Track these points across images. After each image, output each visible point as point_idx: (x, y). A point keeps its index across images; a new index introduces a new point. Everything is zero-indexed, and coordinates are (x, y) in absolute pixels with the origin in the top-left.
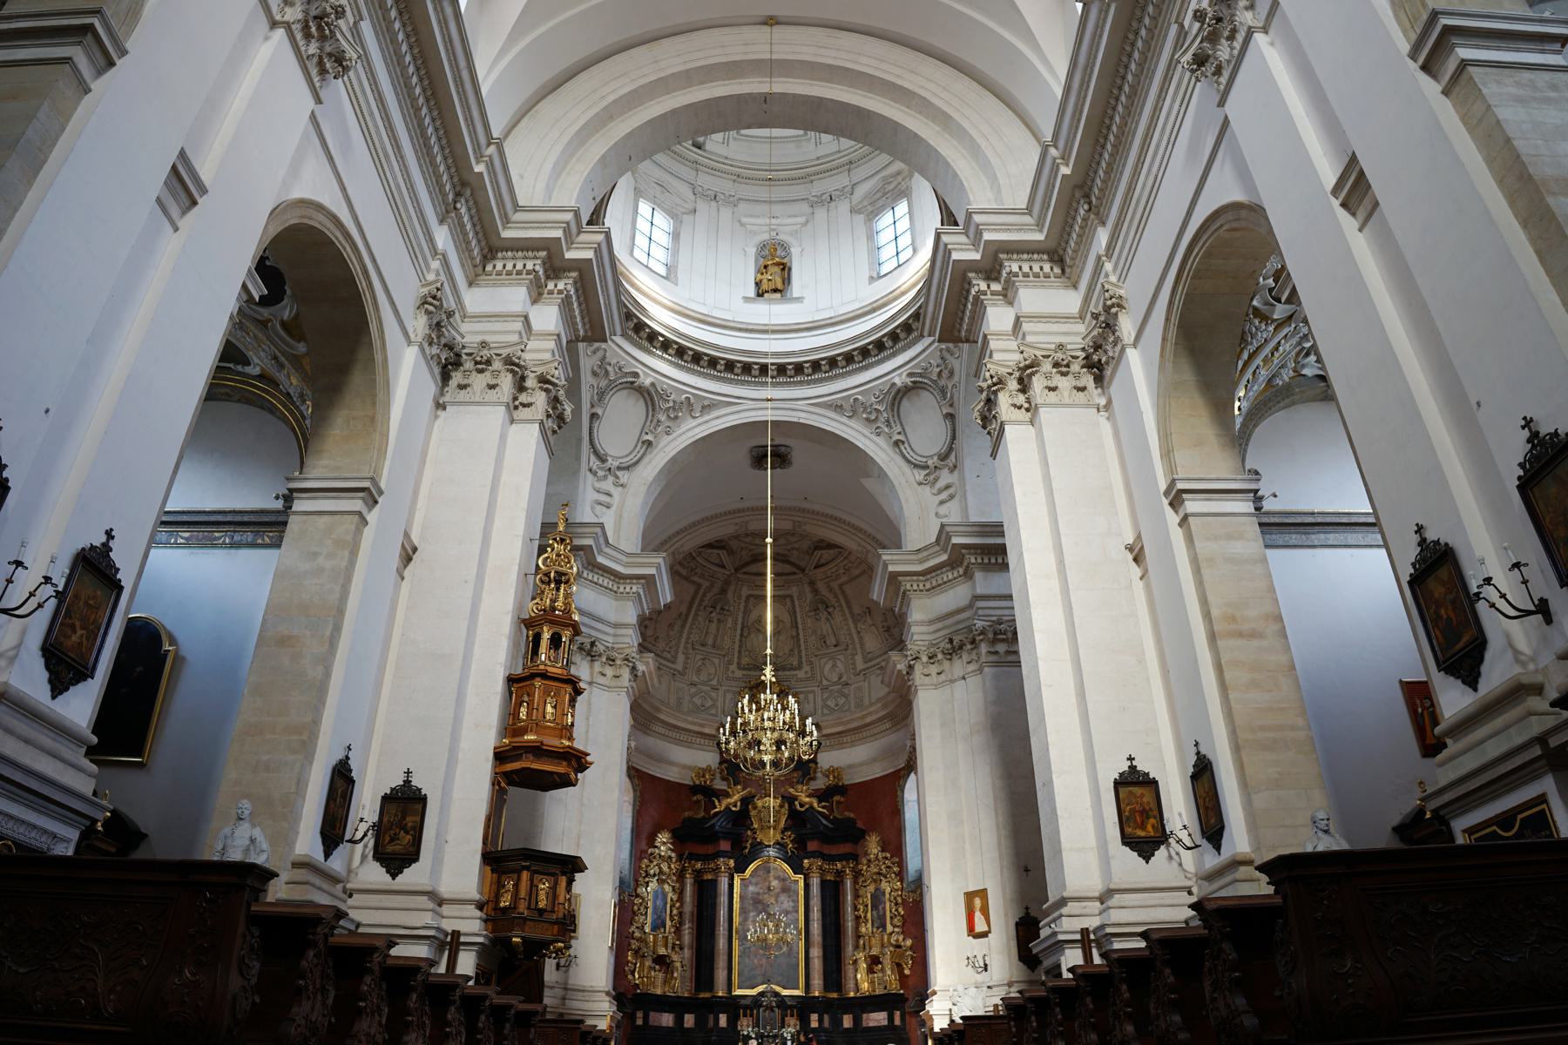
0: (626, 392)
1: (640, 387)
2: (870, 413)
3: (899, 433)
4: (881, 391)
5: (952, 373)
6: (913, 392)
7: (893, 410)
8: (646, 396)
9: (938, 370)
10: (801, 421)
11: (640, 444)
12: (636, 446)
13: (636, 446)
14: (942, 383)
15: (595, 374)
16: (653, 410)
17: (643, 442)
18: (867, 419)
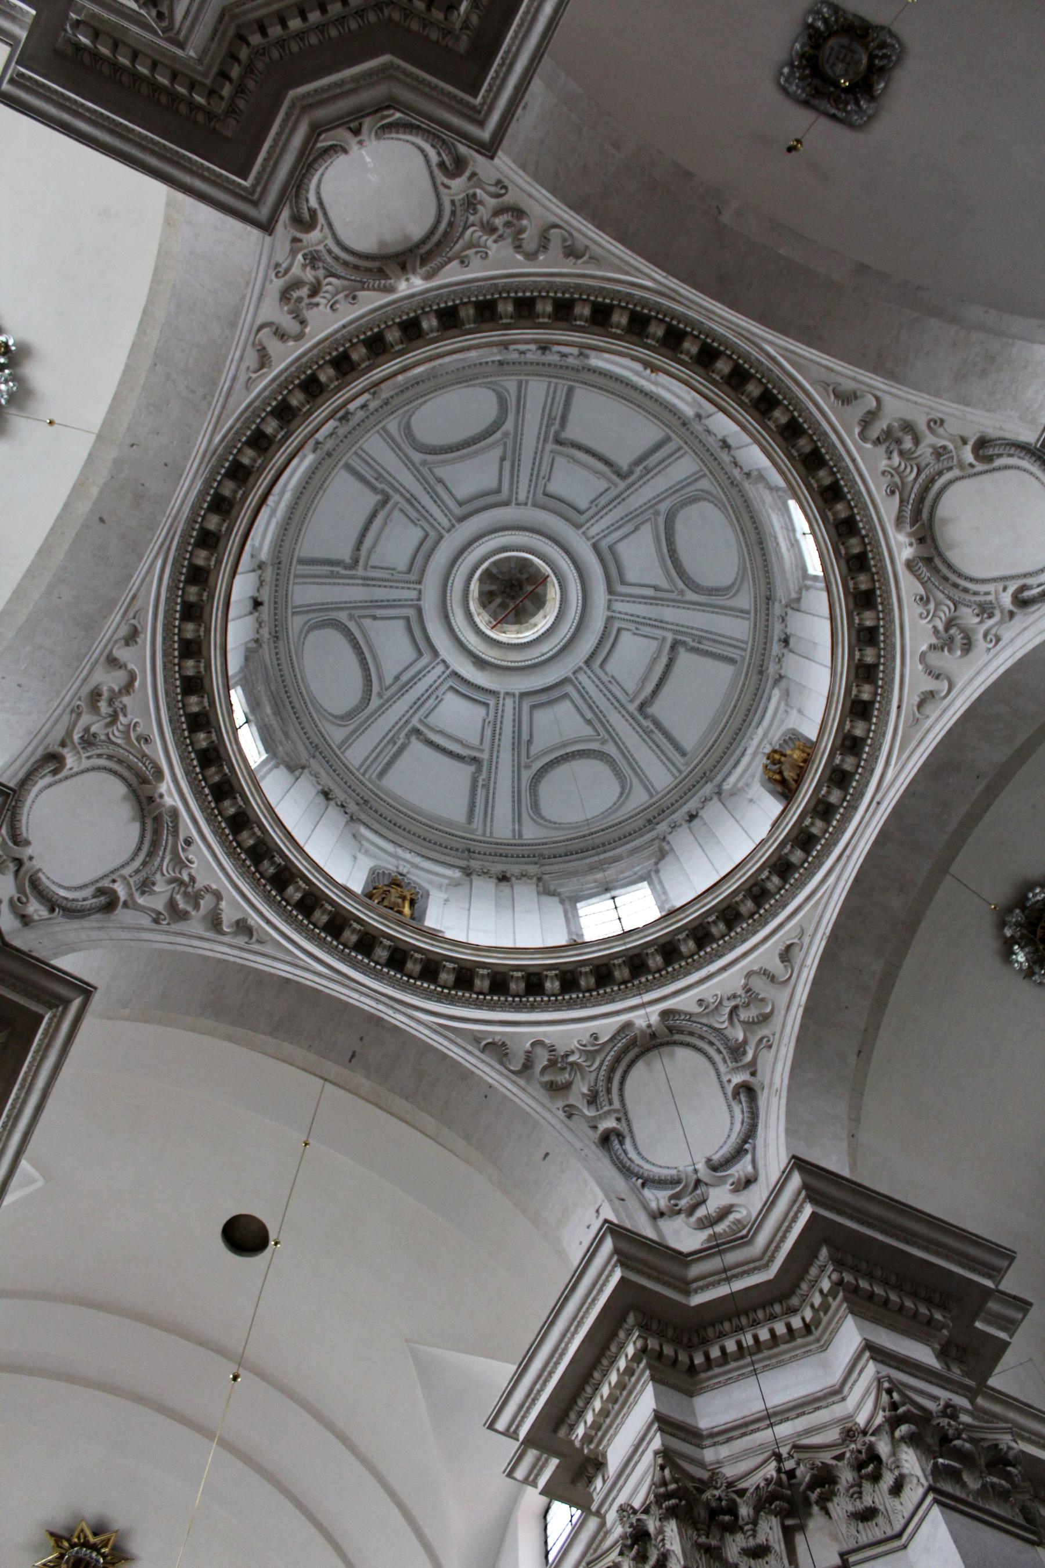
0: (953, 556)
1: (921, 540)
2: (508, 224)
3: (443, 184)
4: (464, 262)
5: (285, 295)
6: (393, 249)
7: (451, 224)
8: (925, 515)
9: (317, 299)
10: (664, 274)
11: (999, 462)
12: (1007, 467)
13: (1007, 467)
14: (309, 275)
15: (968, 646)
16: (932, 481)
17: (990, 459)
18: (518, 212)
